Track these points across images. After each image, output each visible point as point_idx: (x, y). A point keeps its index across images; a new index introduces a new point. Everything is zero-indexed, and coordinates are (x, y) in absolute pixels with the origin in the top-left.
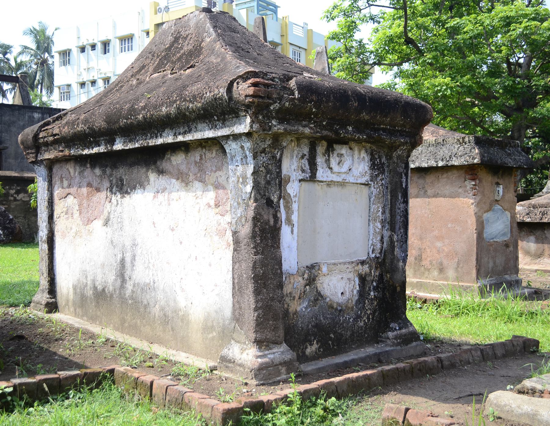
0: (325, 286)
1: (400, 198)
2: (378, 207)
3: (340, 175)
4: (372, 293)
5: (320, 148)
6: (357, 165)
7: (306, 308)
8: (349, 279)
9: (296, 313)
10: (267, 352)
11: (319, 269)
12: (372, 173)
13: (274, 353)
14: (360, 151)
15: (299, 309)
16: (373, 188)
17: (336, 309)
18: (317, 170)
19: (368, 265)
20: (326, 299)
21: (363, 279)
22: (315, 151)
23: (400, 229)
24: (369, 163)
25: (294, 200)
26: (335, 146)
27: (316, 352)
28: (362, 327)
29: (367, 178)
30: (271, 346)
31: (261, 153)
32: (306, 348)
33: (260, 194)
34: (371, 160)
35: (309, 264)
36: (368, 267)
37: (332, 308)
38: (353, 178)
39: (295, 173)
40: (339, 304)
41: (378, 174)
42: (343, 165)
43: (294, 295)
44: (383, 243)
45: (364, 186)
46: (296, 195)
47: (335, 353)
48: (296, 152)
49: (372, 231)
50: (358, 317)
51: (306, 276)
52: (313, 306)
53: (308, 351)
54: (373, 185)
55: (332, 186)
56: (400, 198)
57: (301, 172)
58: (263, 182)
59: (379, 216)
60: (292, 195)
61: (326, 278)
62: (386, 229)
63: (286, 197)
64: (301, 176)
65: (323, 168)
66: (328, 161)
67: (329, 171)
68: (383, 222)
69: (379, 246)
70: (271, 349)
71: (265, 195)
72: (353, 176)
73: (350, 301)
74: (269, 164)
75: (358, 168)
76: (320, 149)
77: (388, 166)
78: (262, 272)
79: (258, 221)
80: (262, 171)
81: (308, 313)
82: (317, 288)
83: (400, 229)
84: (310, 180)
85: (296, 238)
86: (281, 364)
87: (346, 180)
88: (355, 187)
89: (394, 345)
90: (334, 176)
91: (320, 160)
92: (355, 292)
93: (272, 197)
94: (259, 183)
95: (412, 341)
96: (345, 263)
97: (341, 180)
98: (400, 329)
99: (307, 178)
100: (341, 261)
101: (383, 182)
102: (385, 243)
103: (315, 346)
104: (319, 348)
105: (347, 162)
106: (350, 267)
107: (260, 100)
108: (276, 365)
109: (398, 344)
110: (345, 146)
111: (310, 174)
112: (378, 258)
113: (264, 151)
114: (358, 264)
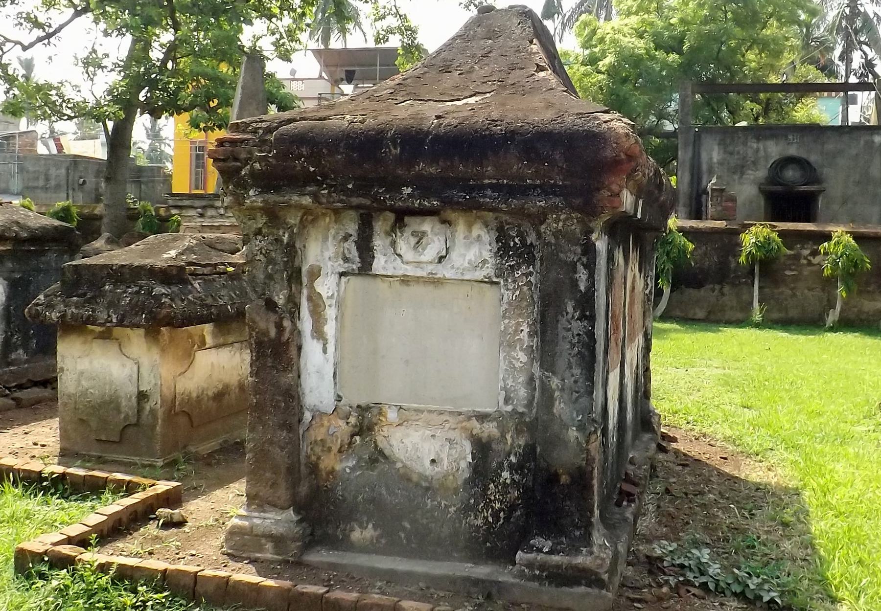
0: (394, 442)
1: (570, 309)
2: (519, 324)
3: (421, 265)
4: (506, 474)
5: (380, 223)
6: (463, 251)
7: (353, 469)
8: (450, 441)
9: (332, 472)
10: (256, 514)
11: (380, 414)
14: (470, 226)
15: (338, 467)
17: (417, 485)
18: (374, 257)
19: (495, 424)
20: (394, 463)
21: (482, 448)
22: (371, 228)
23: (570, 367)
24: (494, 244)
26: (406, 219)
28: (478, 528)
29: (489, 270)
30: (267, 507)
31: (256, 235)
32: (352, 530)
34: (498, 240)
35: (363, 402)
36: (498, 427)
37: (409, 480)
38: (453, 271)
39: (330, 263)
40: (426, 478)
41: (519, 266)
42: (424, 249)
46: (333, 295)
48: (332, 231)
49: (503, 366)
51: (353, 420)
52: (367, 469)
54: (502, 283)
56: (570, 309)
57: (342, 262)
58: (262, 276)
59: (520, 339)
60: (324, 296)
66: (393, 244)
68: (529, 350)
69: (523, 392)
70: (264, 511)
72: (453, 267)
75: (465, 255)
76: (380, 226)
79: (253, 330)
82: (375, 442)
83: (570, 367)
84: (359, 274)
85: (332, 361)
87: (435, 274)
88: (467, 288)
89: (521, 575)
91: (379, 243)
92: (463, 465)
93: (276, 298)
94: (254, 277)
96: (441, 413)
97: (424, 274)
98: (551, 552)
100: (433, 407)
101: (532, 279)
104: (378, 538)
108: (257, 536)
109: (534, 578)
110: (428, 219)
111: (359, 265)
112: (522, 414)
113: (258, 232)
114: (469, 418)
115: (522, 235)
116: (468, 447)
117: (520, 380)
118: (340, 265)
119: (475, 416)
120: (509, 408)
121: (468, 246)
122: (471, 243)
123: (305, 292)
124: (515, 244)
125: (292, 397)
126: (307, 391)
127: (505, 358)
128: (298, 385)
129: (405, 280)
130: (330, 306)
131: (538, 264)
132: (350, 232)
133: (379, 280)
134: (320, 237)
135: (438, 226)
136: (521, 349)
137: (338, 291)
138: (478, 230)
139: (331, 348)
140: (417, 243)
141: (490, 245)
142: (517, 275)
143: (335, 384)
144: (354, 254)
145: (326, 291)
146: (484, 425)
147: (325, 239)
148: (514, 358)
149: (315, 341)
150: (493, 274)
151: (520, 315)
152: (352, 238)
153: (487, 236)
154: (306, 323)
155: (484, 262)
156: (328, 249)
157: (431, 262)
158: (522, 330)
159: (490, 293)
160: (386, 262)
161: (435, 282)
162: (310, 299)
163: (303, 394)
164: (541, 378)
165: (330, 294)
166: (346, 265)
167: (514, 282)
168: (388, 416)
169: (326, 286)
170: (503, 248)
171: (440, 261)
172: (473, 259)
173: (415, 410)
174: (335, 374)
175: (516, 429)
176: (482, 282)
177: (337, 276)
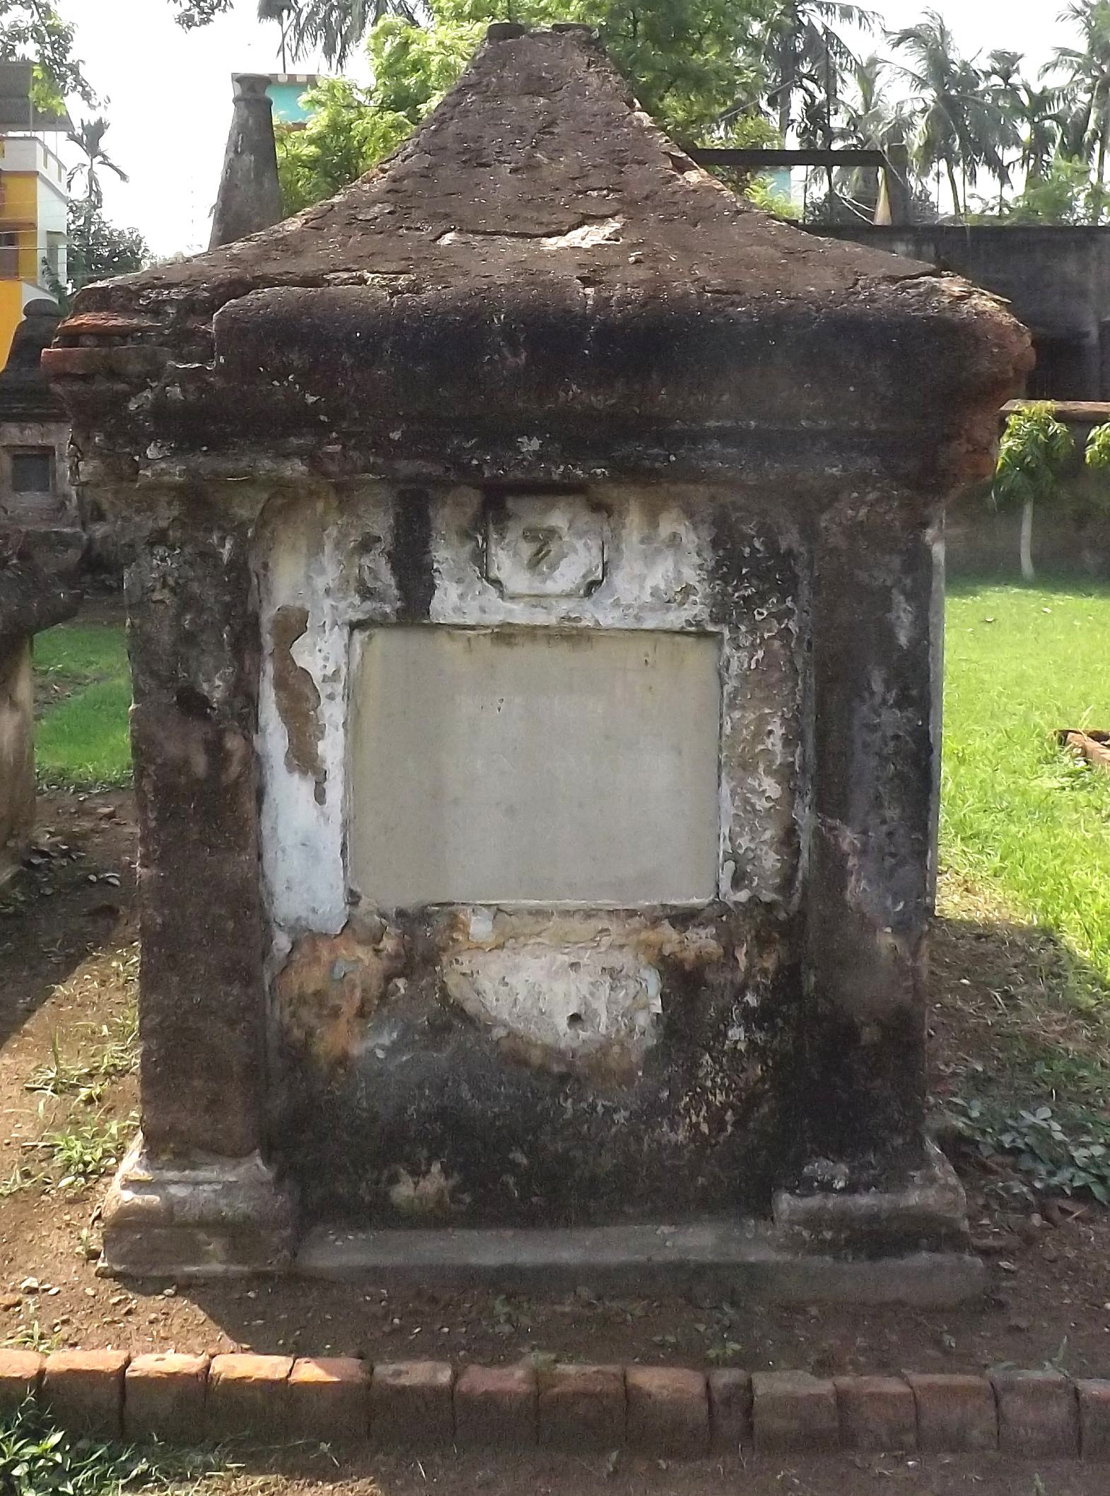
0: (486, 984)
1: (878, 686)
2: (762, 720)
3: (545, 602)
4: (737, 1033)
5: (446, 511)
6: (638, 567)
7: (392, 1050)
8: (613, 973)
9: (343, 1060)
10: (171, 1175)
12: (724, 593)
13: (197, 1184)
15: (357, 1049)
16: (727, 650)
17: (542, 1071)
18: (433, 587)
20: (488, 1029)
21: (683, 981)
22: (426, 523)
23: (877, 803)
24: (708, 554)
25: (324, 690)
26: (510, 503)
27: (440, 1203)
28: (678, 1148)
29: (696, 609)
30: (198, 1155)
31: (151, 545)
32: (394, 1180)
33: (154, 674)
34: (715, 544)
36: (717, 937)
37: (525, 1063)
38: (618, 613)
39: (327, 603)
40: (559, 1055)
41: (762, 598)
42: (553, 567)
43: (334, 1000)
44: (797, 852)
45: (690, 640)
46: (336, 672)
47: (527, 1219)
48: (333, 531)
50: (653, 1111)
51: (388, 944)
52: (426, 1048)
53: (404, 1191)
54: (727, 634)
55: (519, 640)
56: (878, 686)
57: (357, 600)
58: (166, 638)
59: (766, 751)
60: (316, 675)
61: (490, 957)
62: (808, 799)
63: (291, 681)
64: (355, 608)
65: (459, 581)
66: (481, 558)
67: (492, 592)
68: (786, 774)
69: (771, 860)
70: (194, 1167)
71: (173, 678)
72: (616, 604)
73: (616, 1049)
74: (188, 580)
75: (642, 578)
76: (445, 519)
77: (810, 566)
78: (159, 920)
79: (151, 760)
80: (162, 602)
81: (402, 1067)
82: (443, 989)
83: (877, 803)
85: (337, 818)
86: (202, 1224)
87: (577, 619)
88: (646, 646)
89: (795, 1244)
90: (517, 607)
91: (445, 555)
92: (642, 1020)
93: (205, 686)
94: (149, 640)
95: (916, 1248)
96: (589, 914)
97: (552, 620)
98: (851, 1189)
99: (385, 615)
100: (571, 903)
102: (805, 855)
103: (435, 1181)
104: (455, 1190)
105: (572, 557)
106: (614, 927)
107: (77, 387)
108: (184, 1225)
109: (821, 1247)
110: (562, 501)
111: (399, 604)
112: (770, 906)
113: (159, 538)
114: (655, 922)
115: (769, 534)
116: (653, 982)
117: (767, 835)
118: (352, 605)
119: (668, 917)
120: (743, 896)
121: (649, 559)
122: (658, 551)
123: (269, 668)
124: (754, 550)
125: (250, 906)
126: (279, 887)
127: (733, 793)
128: (260, 875)
129: (505, 635)
130: (331, 697)
131: (805, 591)
132: (377, 530)
133: (442, 638)
134: (303, 544)
135: (586, 519)
136: (768, 772)
137: (348, 664)
138: (669, 524)
139: (335, 791)
140: (538, 553)
141: (699, 555)
142: (758, 618)
143: (345, 867)
144: (387, 578)
145: (321, 663)
146: (688, 934)
147: (316, 548)
148: (753, 791)
149: (296, 776)
150: (706, 616)
151: (767, 700)
152: (380, 546)
153: (693, 536)
154: (274, 738)
155: (687, 591)
156: (322, 571)
157: (568, 595)
158: (771, 732)
159: (698, 658)
160: (461, 596)
161: (572, 635)
162: (281, 684)
163: (271, 894)
164: (817, 833)
165: (330, 671)
166: (368, 605)
167: (752, 631)
168: (472, 930)
169: (319, 654)
170: (727, 563)
171: (588, 593)
172: (662, 587)
173: (530, 913)
174: (344, 844)
175: (757, 937)
176: (681, 632)
177: (346, 630)
